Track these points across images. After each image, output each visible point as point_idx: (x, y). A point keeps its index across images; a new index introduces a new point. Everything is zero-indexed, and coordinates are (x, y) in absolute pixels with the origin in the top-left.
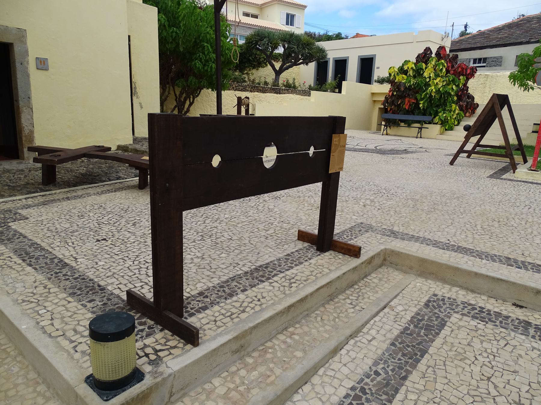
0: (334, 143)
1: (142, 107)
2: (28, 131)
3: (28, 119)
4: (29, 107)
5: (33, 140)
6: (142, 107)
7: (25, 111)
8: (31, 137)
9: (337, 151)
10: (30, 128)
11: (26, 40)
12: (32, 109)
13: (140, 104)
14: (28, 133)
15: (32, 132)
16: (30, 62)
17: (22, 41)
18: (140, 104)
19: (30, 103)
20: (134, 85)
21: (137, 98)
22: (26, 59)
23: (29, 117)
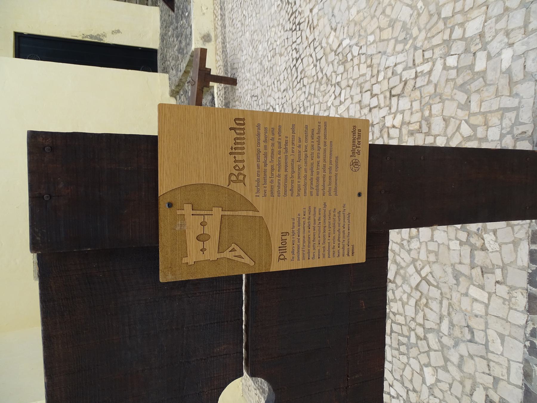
0: (212, 254)
1: (118, 31)
6: (118, 31)
9: (260, 203)
13: (113, 32)
18: (113, 32)
20: (87, 37)
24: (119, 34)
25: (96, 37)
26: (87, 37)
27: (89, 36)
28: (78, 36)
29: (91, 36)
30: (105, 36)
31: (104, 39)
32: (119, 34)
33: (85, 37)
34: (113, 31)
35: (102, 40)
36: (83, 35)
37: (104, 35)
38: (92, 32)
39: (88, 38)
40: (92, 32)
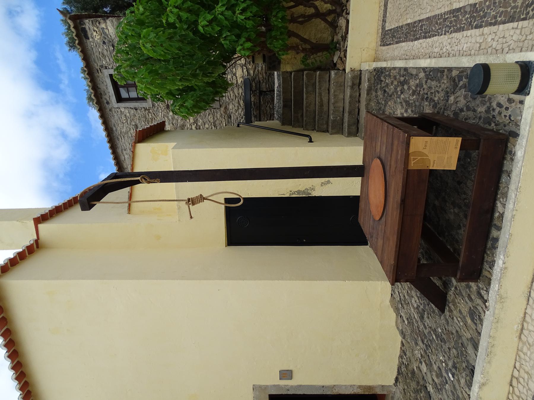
2: (359, 389)
3: (346, 388)
4: (333, 387)
5: (370, 386)
7: (337, 391)
8: (365, 388)
10: (355, 388)
11: (264, 386)
12: (335, 386)
14: (361, 390)
15: (360, 387)
16: (286, 384)
17: (265, 388)
19: (328, 387)
20: (294, 194)
21: (313, 189)
22: (283, 386)
23: (344, 387)
24: (329, 185)
25: (304, 192)
26: (294, 193)
27: (296, 192)
28: (285, 194)
29: (299, 192)
30: (313, 189)
31: (312, 193)
32: (329, 185)
33: (293, 194)
34: (322, 183)
35: (310, 194)
36: (291, 191)
37: (313, 189)
38: (300, 188)
39: (295, 194)
40: (300, 188)
